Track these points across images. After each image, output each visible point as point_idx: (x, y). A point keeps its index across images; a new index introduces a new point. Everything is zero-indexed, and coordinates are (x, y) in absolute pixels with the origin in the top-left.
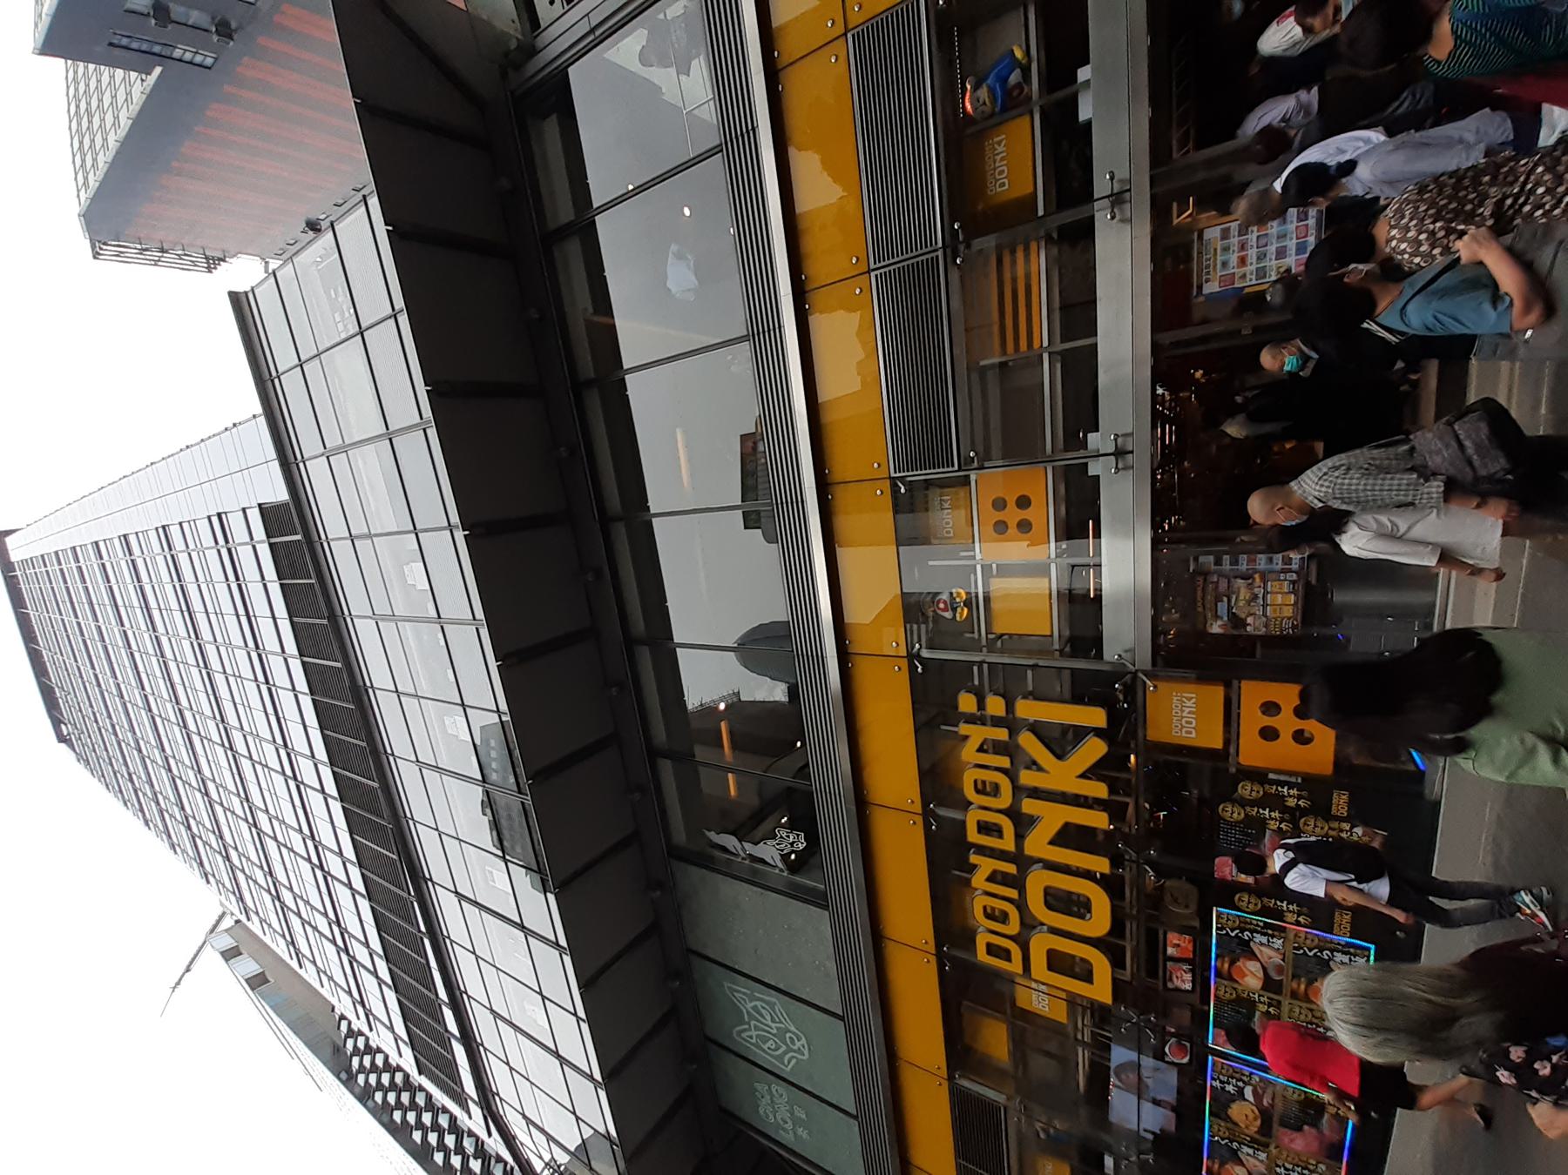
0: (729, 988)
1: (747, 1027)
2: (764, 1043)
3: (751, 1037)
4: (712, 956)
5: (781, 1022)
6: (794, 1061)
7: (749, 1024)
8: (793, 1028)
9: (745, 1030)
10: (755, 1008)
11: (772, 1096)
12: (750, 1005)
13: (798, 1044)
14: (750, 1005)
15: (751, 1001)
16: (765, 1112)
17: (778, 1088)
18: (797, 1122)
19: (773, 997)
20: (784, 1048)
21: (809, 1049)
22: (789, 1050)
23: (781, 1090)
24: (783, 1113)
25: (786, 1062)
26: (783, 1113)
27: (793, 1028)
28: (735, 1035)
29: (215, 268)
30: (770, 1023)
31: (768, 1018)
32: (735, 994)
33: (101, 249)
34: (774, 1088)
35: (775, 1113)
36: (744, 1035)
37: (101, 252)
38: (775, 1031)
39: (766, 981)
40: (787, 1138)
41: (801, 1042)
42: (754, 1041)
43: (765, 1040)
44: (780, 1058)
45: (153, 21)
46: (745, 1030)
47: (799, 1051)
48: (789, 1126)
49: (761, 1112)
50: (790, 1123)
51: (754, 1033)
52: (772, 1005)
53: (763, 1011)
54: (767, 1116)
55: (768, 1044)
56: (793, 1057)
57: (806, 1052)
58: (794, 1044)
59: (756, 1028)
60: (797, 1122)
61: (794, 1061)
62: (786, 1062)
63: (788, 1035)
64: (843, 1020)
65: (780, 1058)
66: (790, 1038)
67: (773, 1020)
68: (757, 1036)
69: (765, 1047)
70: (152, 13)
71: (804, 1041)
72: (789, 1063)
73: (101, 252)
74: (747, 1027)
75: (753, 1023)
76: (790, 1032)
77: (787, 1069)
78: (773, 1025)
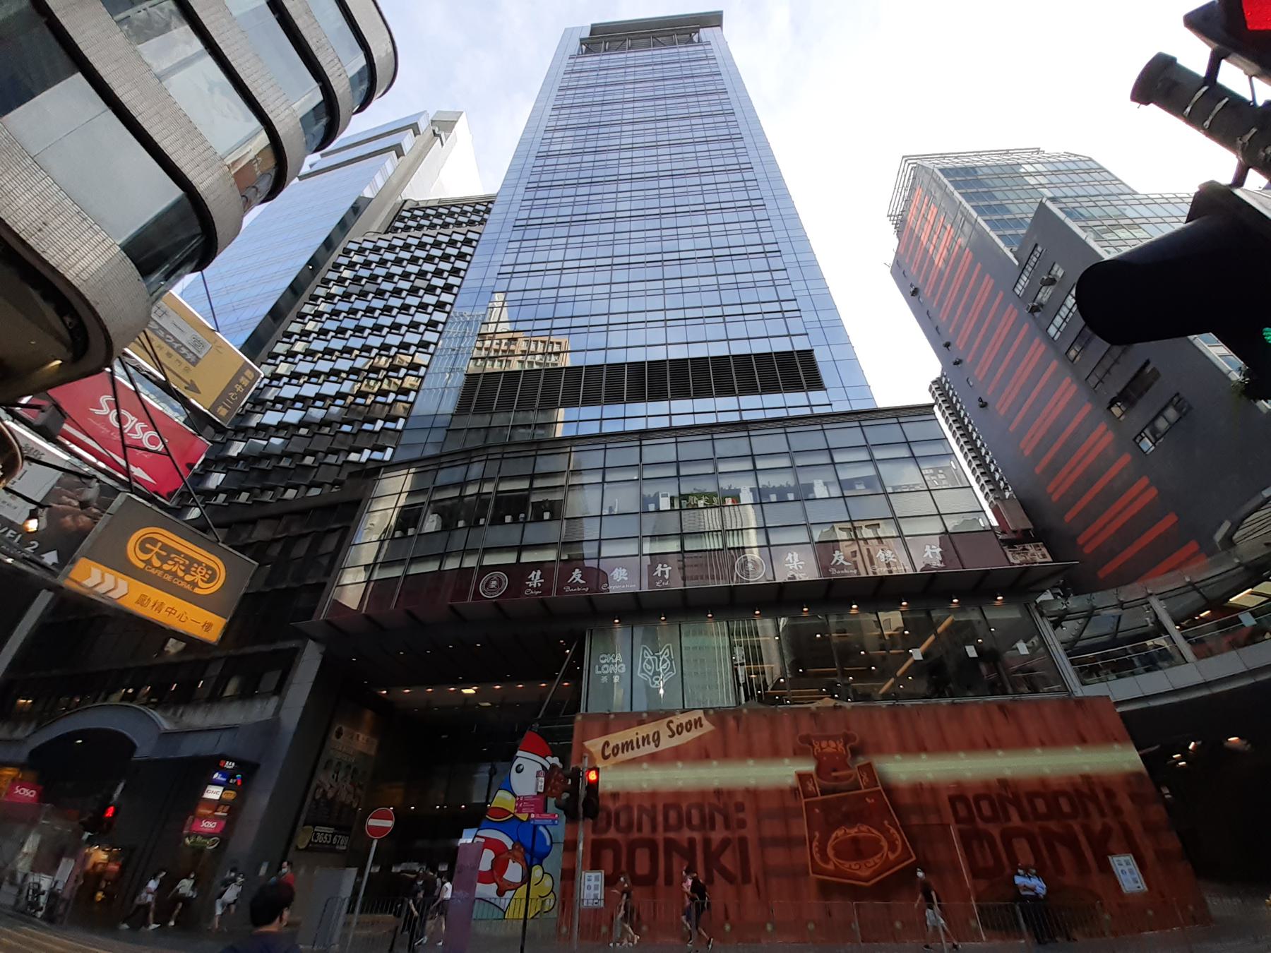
7: (654, 655)
22: (652, 677)
29: (895, 228)
33: (909, 164)
35: (607, 663)
36: (645, 651)
37: (907, 164)
43: (649, 662)
45: (1045, 278)
47: (653, 683)
53: (666, 664)
54: (603, 659)
55: (648, 666)
59: (654, 660)
69: (645, 663)
70: (1050, 277)
73: (907, 164)
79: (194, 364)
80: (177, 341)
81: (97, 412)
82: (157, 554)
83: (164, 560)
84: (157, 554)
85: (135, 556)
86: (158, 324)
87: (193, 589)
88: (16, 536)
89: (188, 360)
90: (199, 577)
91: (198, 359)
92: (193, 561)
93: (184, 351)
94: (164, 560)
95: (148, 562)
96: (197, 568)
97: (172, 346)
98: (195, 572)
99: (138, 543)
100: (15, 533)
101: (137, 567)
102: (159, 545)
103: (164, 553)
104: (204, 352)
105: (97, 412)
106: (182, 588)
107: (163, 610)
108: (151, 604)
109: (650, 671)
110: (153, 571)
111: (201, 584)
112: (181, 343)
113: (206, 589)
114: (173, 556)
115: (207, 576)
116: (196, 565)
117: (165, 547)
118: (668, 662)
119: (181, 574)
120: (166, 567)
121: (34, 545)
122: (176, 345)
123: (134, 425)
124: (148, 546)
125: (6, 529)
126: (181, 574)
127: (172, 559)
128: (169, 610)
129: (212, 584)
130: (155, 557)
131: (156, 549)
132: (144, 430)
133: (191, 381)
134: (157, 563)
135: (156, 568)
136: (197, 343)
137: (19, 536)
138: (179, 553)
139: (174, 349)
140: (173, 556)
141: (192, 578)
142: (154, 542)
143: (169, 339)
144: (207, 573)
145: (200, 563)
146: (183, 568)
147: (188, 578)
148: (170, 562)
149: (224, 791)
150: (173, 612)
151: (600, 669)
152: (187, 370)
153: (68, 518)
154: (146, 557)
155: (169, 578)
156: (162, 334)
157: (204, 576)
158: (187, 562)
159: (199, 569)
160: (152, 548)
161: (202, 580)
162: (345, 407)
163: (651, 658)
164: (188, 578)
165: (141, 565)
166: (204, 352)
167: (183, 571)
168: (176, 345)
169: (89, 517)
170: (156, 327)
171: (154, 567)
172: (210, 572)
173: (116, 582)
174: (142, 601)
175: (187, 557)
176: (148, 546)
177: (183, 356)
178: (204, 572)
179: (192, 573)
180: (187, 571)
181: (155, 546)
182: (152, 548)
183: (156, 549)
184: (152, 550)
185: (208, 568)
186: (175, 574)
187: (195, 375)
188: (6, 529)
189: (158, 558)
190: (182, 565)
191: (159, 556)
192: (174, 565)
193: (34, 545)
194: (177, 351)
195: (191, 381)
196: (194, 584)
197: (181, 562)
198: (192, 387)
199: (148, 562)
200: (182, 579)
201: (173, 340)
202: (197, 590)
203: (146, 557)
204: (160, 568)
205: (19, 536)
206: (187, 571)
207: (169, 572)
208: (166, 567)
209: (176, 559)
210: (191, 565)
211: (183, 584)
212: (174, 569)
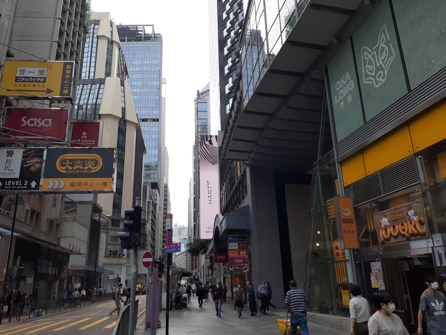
0: (384, 29)
1: (371, 51)
2: (369, 64)
3: (367, 56)
4: (394, 8)
5: (385, 65)
6: (371, 82)
7: (373, 51)
8: (386, 72)
9: (368, 52)
10: (383, 49)
11: (348, 83)
12: (382, 45)
13: (380, 79)
14: (382, 45)
15: (385, 44)
16: (338, 85)
17: (353, 84)
18: (345, 100)
19: (395, 52)
20: (373, 74)
21: (382, 85)
22: (374, 77)
23: (353, 86)
24: (344, 92)
25: (367, 80)
26: (344, 92)
27: (386, 72)
28: (362, 49)
30: (380, 60)
31: (383, 58)
32: (383, 34)
34: (352, 81)
35: (342, 88)
36: (366, 53)
38: (378, 65)
39: (402, 43)
40: (336, 101)
41: (382, 80)
42: (366, 59)
43: (371, 63)
44: (367, 76)
46: (368, 52)
47: (377, 82)
48: (341, 98)
49: (338, 83)
50: (342, 97)
51: (370, 56)
52: (391, 54)
53: (384, 53)
54: (338, 87)
55: (369, 66)
56: (372, 81)
57: (379, 85)
58: (379, 77)
59: (373, 56)
60: (345, 100)
61: (371, 82)
62: (367, 80)
63: (381, 72)
64: (409, 93)
65: (367, 76)
66: (380, 74)
67: (383, 61)
68: (370, 59)
69: (367, 66)
71: (383, 81)
72: (369, 80)
74: (371, 51)
75: (375, 52)
76: (384, 71)
77: (364, 81)
78: (381, 62)
79: (45, 82)
80: (33, 78)
81: (23, 125)
83: (72, 166)
85: (61, 169)
86: (23, 77)
87: (90, 171)
88: (19, 182)
89: (42, 82)
90: (90, 166)
91: (45, 78)
92: (84, 160)
93: (38, 79)
94: (72, 166)
95: (67, 169)
96: (87, 163)
97: (33, 81)
98: (88, 164)
99: (98, 160)
100: (18, 181)
102: (68, 160)
104: (46, 73)
105: (23, 125)
107: (82, 185)
108: (76, 185)
109: (371, 71)
112: (35, 77)
113: (95, 169)
114: (75, 162)
115: (94, 164)
116: (86, 162)
117: (70, 160)
118: (386, 48)
119: (82, 168)
120: (74, 168)
121: (26, 182)
122: (34, 80)
123: (37, 122)
124: (64, 163)
125: (15, 181)
126: (82, 168)
127: (76, 164)
128: (85, 184)
129: (98, 165)
130: (68, 166)
131: (67, 163)
132: (41, 121)
133: (47, 89)
134: (70, 168)
135: (71, 170)
136: (41, 72)
137: (20, 181)
138: (77, 160)
139: (34, 82)
140: (75, 162)
141: (88, 167)
142: (65, 160)
143: (31, 80)
144: (93, 162)
145: (88, 160)
146: (81, 165)
147: (86, 168)
148: (75, 165)
149: (239, 244)
150: (87, 184)
151: (338, 98)
152: (43, 86)
153: (32, 168)
154: (65, 168)
155: (78, 171)
156: (27, 80)
157: (92, 164)
158: (82, 162)
159: (89, 162)
160: (66, 163)
161: (92, 166)
162: (155, 36)
163: (370, 56)
164: (86, 168)
165: (65, 172)
166: (46, 73)
168: (34, 80)
169: (39, 163)
170: (24, 79)
171: (69, 170)
172: (94, 161)
173: (59, 182)
174: (72, 185)
175: (81, 160)
176: (64, 163)
177: (39, 81)
178: (91, 162)
179: (86, 165)
181: (67, 162)
182: (66, 163)
184: (66, 164)
185: (92, 160)
186: (80, 169)
187: (48, 85)
188: (15, 181)
189: (70, 166)
190: (80, 164)
191: (69, 165)
192: (78, 165)
193: (26, 182)
194: (36, 81)
195: (47, 89)
197: (80, 163)
198: (49, 91)
199: (67, 169)
200: (83, 169)
201: (32, 79)
202: (92, 171)
203: (65, 168)
204: (73, 169)
205: (20, 181)
206: (84, 166)
207: (77, 169)
208: (74, 168)
209: (77, 163)
210: (84, 162)
211: (85, 171)
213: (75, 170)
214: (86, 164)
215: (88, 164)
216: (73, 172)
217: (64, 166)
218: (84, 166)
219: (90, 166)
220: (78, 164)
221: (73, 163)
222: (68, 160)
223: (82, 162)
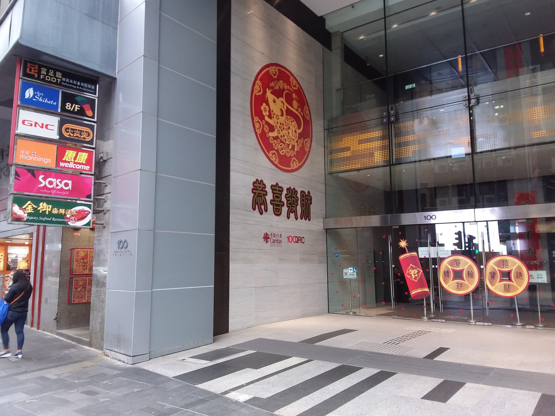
82: (71, 132)
83: (73, 133)
84: (71, 132)
98: (83, 134)
101: (68, 138)
102: (70, 129)
103: (72, 131)
106: (81, 140)
110: (72, 137)
111: (86, 138)
114: (75, 131)
115: (87, 135)
116: (82, 132)
117: (72, 129)
119: (80, 136)
120: (75, 135)
124: (67, 130)
126: (80, 136)
127: (75, 132)
134: (72, 135)
138: (76, 130)
140: (75, 131)
142: (68, 129)
144: (87, 134)
145: (83, 131)
146: (79, 134)
147: (82, 137)
148: (75, 133)
154: (68, 134)
158: (80, 132)
159: (84, 133)
164: (82, 137)
165: (68, 137)
167: (80, 135)
171: (71, 136)
175: (79, 130)
176: (67, 130)
180: (81, 135)
183: (70, 131)
185: (86, 132)
186: (78, 137)
196: (85, 138)
199: (70, 135)
200: (80, 137)
202: (86, 140)
203: (68, 134)
204: (73, 136)
207: (76, 136)
211: (81, 139)
212: (77, 135)
213: (75, 137)
214: (82, 134)
215: (83, 134)
216: (74, 137)
217: (68, 132)
218: (81, 135)
219: (85, 136)
220: (77, 133)
221: (74, 131)
222: (70, 129)
223: (80, 132)
